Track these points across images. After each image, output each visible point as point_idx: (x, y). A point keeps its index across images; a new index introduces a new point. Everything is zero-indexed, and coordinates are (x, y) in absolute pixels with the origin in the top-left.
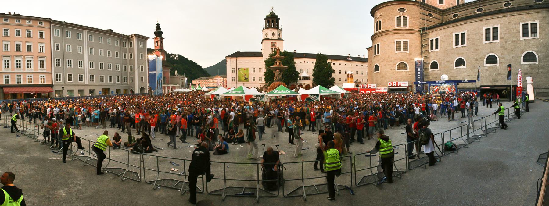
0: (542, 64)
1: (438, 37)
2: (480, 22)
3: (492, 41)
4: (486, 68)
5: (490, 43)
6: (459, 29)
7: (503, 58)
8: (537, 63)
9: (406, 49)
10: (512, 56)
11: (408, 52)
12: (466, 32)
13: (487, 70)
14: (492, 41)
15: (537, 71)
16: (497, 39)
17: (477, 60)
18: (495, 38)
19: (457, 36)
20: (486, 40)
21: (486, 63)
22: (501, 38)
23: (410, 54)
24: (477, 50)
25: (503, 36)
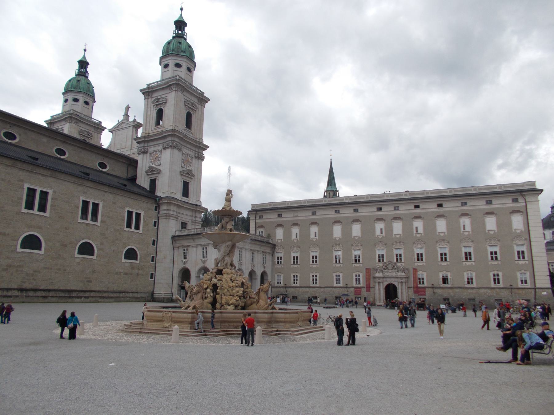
0: (143, 264)
4: (78, 260)
5: (87, 224)
8: (138, 262)
13: (79, 264)
14: (89, 221)
15: (137, 271)
17: (64, 245)
21: (79, 253)
22: (102, 222)
24: (66, 228)
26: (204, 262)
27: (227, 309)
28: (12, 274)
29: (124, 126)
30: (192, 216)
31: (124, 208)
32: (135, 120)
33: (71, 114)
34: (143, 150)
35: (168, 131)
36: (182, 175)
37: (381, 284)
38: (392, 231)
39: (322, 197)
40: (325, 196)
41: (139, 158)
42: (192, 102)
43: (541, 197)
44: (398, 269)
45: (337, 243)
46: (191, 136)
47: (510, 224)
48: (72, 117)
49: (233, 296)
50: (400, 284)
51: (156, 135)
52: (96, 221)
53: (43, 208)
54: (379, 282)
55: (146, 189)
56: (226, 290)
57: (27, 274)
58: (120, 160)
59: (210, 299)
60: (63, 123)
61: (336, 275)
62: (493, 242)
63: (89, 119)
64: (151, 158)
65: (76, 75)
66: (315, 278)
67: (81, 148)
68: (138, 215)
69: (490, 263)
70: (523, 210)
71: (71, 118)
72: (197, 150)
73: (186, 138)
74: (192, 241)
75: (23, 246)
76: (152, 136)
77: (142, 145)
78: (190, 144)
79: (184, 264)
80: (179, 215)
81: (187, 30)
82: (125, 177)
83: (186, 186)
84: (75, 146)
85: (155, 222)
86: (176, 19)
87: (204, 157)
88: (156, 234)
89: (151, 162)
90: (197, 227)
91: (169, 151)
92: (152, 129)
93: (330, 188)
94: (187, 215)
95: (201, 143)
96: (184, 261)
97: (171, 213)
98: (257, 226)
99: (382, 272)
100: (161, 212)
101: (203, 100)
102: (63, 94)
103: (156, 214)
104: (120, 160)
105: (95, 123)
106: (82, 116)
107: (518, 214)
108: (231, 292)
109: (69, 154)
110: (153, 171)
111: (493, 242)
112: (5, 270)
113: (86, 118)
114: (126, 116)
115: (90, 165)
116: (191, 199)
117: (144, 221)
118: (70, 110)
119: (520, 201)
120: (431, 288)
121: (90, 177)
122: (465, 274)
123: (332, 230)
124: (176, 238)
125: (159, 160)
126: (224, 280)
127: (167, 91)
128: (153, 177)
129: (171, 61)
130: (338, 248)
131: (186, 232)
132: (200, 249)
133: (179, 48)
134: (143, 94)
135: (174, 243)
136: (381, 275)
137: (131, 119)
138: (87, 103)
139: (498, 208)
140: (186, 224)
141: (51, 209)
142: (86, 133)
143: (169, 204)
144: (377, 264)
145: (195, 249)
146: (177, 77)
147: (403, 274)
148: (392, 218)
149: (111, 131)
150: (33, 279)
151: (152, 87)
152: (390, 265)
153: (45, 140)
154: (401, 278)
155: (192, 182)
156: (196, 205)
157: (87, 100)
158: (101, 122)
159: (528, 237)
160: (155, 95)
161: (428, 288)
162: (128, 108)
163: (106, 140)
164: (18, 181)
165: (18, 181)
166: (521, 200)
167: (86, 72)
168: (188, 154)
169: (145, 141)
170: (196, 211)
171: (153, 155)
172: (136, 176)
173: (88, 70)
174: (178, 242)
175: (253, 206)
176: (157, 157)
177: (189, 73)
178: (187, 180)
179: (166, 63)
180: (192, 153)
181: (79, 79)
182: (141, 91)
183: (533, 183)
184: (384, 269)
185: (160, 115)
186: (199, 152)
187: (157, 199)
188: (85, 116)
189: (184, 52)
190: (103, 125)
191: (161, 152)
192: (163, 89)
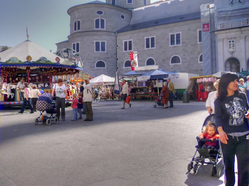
1: (132, 40)
3: (175, 45)
4: (172, 67)
5: (174, 47)
7: (185, 58)
9: (103, 49)
10: (191, 56)
11: (106, 52)
12: (155, 36)
13: (172, 68)
16: (180, 44)
18: (178, 42)
19: (148, 40)
20: (171, 44)
21: (172, 63)
22: (182, 43)
23: (107, 54)
24: (164, 52)
31: (196, 30)
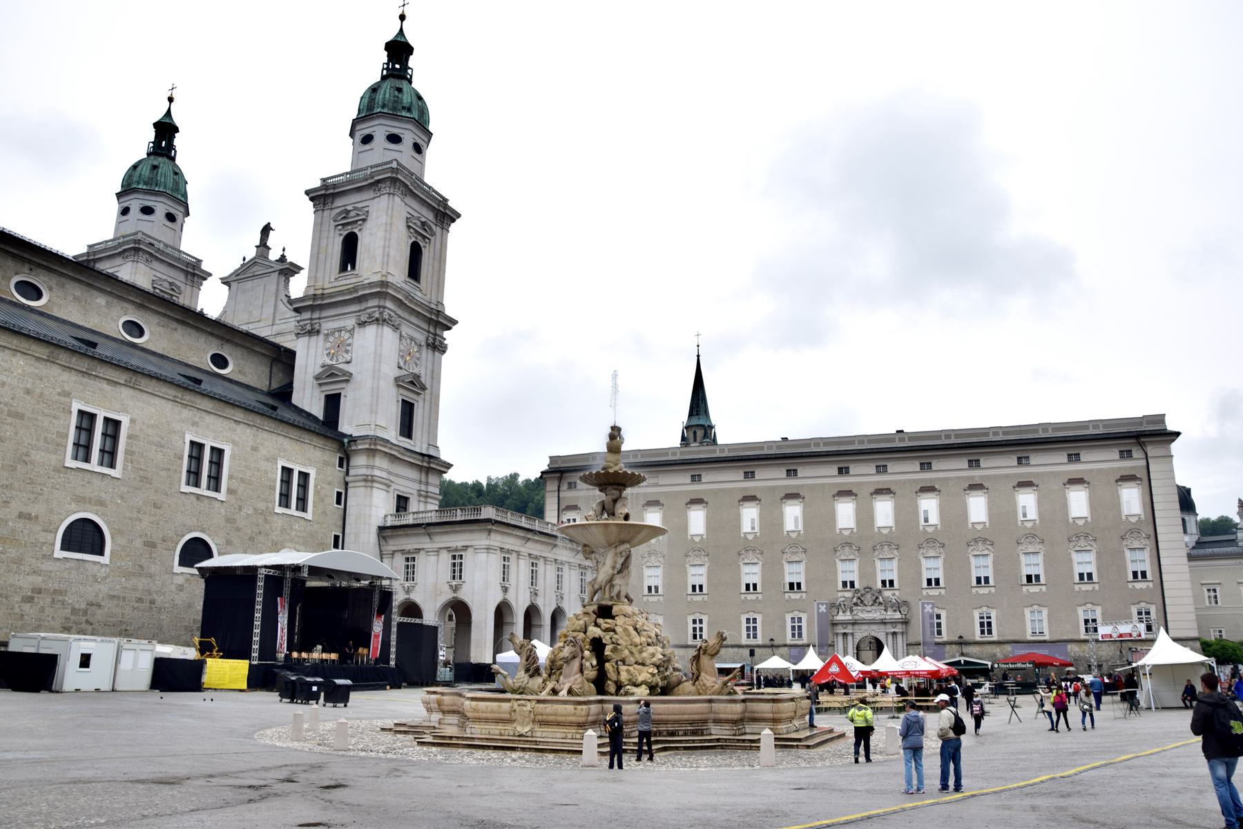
2: (178, 409)
4: (179, 580)
5: (198, 497)
6: (108, 400)
13: (180, 588)
14: (203, 490)
17: (151, 545)
21: (181, 564)
24: (155, 506)
25: (235, 484)
26: (455, 589)
27: (633, 694)
28: (42, 610)
29: (258, 270)
30: (420, 482)
31: (273, 460)
32: (283, 256)
33: (139, 242)
34: (309, 327)
35: (371, 285)
36: (399, 386)
37: (850, 638)
38: (872, 519)
39: (677, 442)
40: (683, 438)
41: (301, 347)
42: (423, 219)
43: (1175, 447)
44: (886, 605)
45: (748, 547)
46: (418, 296)
47: (1116, 503)
48: (140, 249)
49: (643, 664)
50: (890, 637)
51: (341, 293)
52: (217, 489)
53: (109, 456)
54: (845, 635)
55: (315, 418)
56: (627, 652)
57: (74, 611)
58: (257, 349)
59: (592, 674)
60: (119, 261)
61: (748, 620)
62: (1082, 543)
63: (176, 254)
64: (329, 345)
65: (148, 154)
66: (698, 626)
67: (178, 321)
68: (304, 476)
69: (1077, 587)
70: (1142, 474)
71: (137, 250)
72: (432, 330)
73: (411, 301)
74: (427, 539)
75: (64, 547)
76: (331, 295)
77: (307, 315)
78: (418, 314)
79: (408, 591)
80: (392, 478)
81: (412, 61)
82: (265, 389)
83: (408, 410)
84: (164, 315)
85: (339, 494)
86: (390, 37)
87: (446, 347)
88: (341, 523)
89: (328, 354)
90: (431, 507)
91: (371, 330)
92: (332, 279)
93: (695, 421)
94: (408, 479)
95: (439, 313)
96: (407, 584)
97: (377, 473)
98: (563, 506)
99: (852, 611)
100: (352, 472)
101: (445, 215)
102: (119, 195)
103: (342, 475)
104: (257, 349)
105: (188, 264)
106: (161, 246)
107: (1133, 484)
108: (639, 658)
109: (151, 333)
110: (332, 375)
111: (1082, 543)
112: (29, 600)
113: (169, 251)
114: (263, 246)
115: (194, 360)
116: (418, 443)
117: (317, 492)
118: (136, 233)
119: (1135, 455)
120: (956, 643)
121: (203, 386)
122: (1080, 611)
123: (738, 518)
124: (388, 533)
125: (347, 352)
126: (618, 629)
127: (369, 194)
128: (332, 389)
129: (380, 129)
130: (751, 557)
131: (410, 520)
132: (446, 558)
133: (397, 101)
134: (311, 199)
135: (383, 542)
136: (846, 617)
137: (274, 255)
138: (171, 217)
139: (1092, 471)
140: (406, 499)
141: (126, 460)
142: (166, 285)
143: (372, 452)
144: (840, 594)
145: (433, 558)
146: (394, 165)
147: (898, 615)
148: (872, 490)
149: (226, 281)
150: (87, 622)
151: (334, 186)
152: (869, 596)
153: (101, 300)
154: (894, 623)
155: (421, 403)
156: (430, 457)
157: (173, 211)
158: (200, 261)
159: (1152, 533)
160: (339, 202)
161: (951, 643)
162: (266, 230)
163: (212, 300)
164: (59, 394)
165: (59, 394)
166: (1137, 453)
167: (171, 147)
168: (412, 339)
169: (313, 307)
170: (428, 470)
171: (331, 339)
172: (290, 385)
173: (176, 142)
174: (391, 542)
175: (553, 459)
176: (342, 342)
177: (416, 155)
178: (410, 397)
179: (367, 132)
180: (421, 337)
181: (155, 163)
182: (307, 193)
183: (1160, 418)
184: (856, 604)
185: (350, 248)
186: (435, 335)
187: (346, 440)
188: (166, 246)
189: (409, 110)
190: (204, 267)
191: (351, 331)
192: (359, 189)
